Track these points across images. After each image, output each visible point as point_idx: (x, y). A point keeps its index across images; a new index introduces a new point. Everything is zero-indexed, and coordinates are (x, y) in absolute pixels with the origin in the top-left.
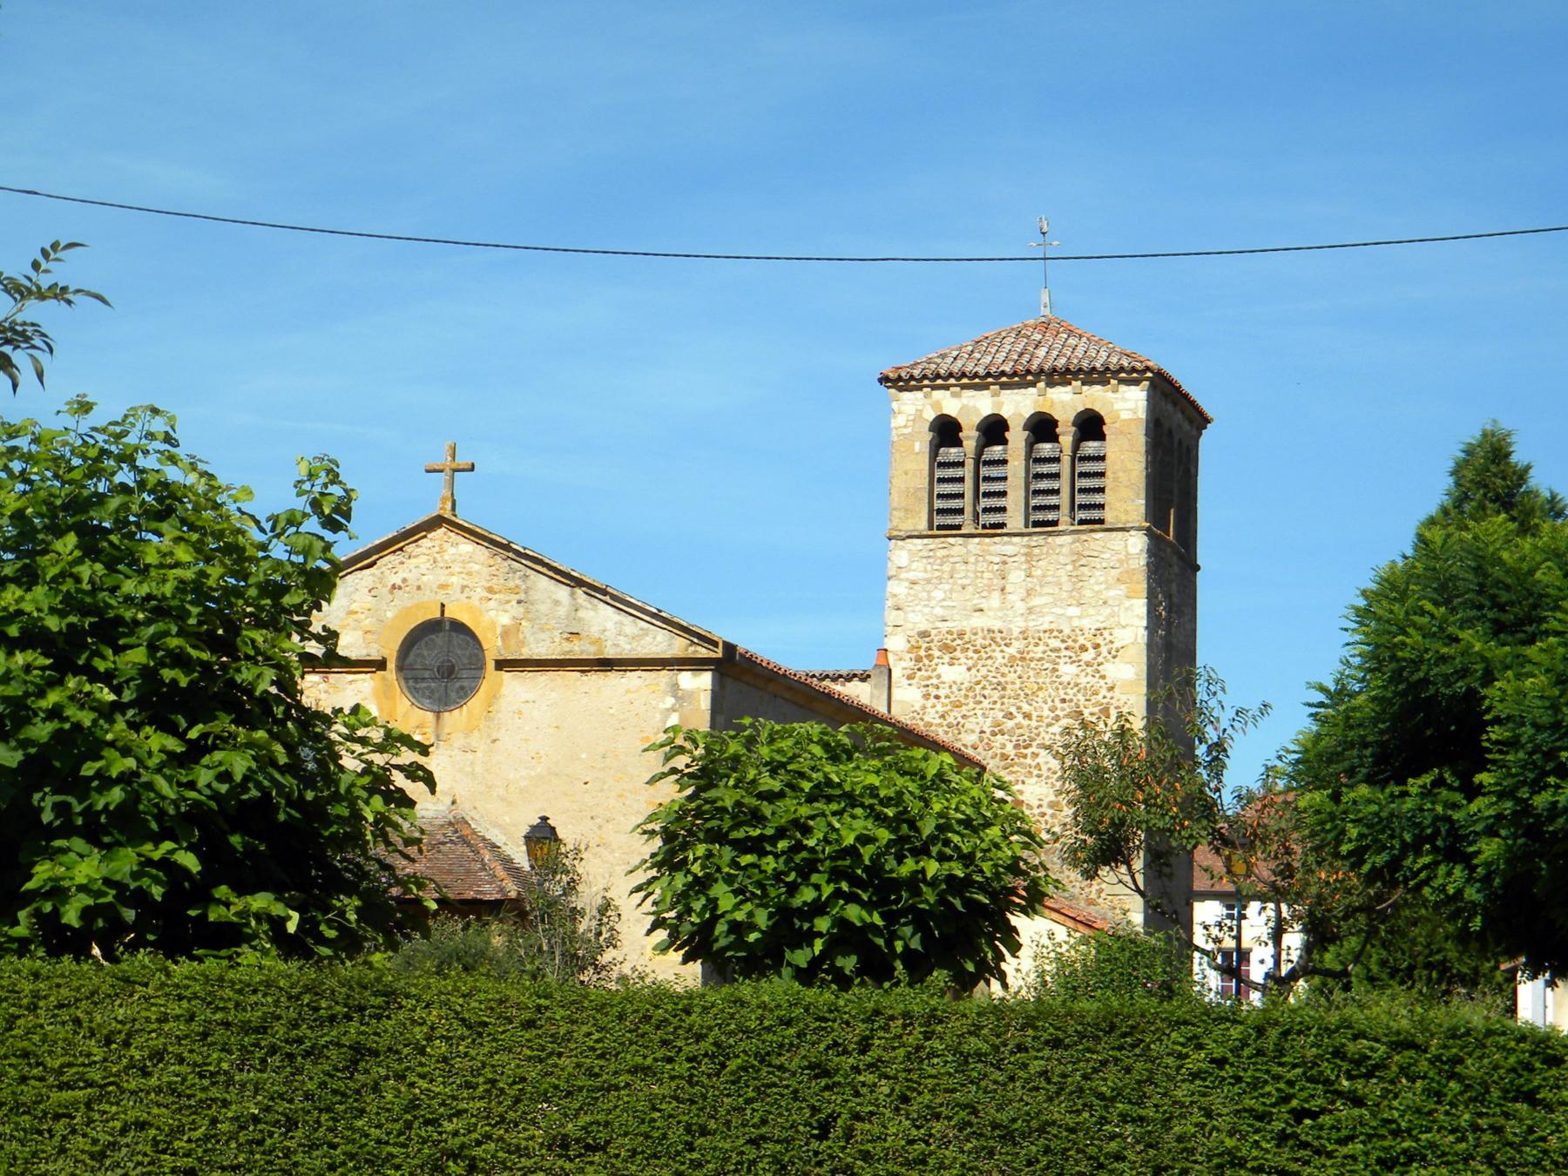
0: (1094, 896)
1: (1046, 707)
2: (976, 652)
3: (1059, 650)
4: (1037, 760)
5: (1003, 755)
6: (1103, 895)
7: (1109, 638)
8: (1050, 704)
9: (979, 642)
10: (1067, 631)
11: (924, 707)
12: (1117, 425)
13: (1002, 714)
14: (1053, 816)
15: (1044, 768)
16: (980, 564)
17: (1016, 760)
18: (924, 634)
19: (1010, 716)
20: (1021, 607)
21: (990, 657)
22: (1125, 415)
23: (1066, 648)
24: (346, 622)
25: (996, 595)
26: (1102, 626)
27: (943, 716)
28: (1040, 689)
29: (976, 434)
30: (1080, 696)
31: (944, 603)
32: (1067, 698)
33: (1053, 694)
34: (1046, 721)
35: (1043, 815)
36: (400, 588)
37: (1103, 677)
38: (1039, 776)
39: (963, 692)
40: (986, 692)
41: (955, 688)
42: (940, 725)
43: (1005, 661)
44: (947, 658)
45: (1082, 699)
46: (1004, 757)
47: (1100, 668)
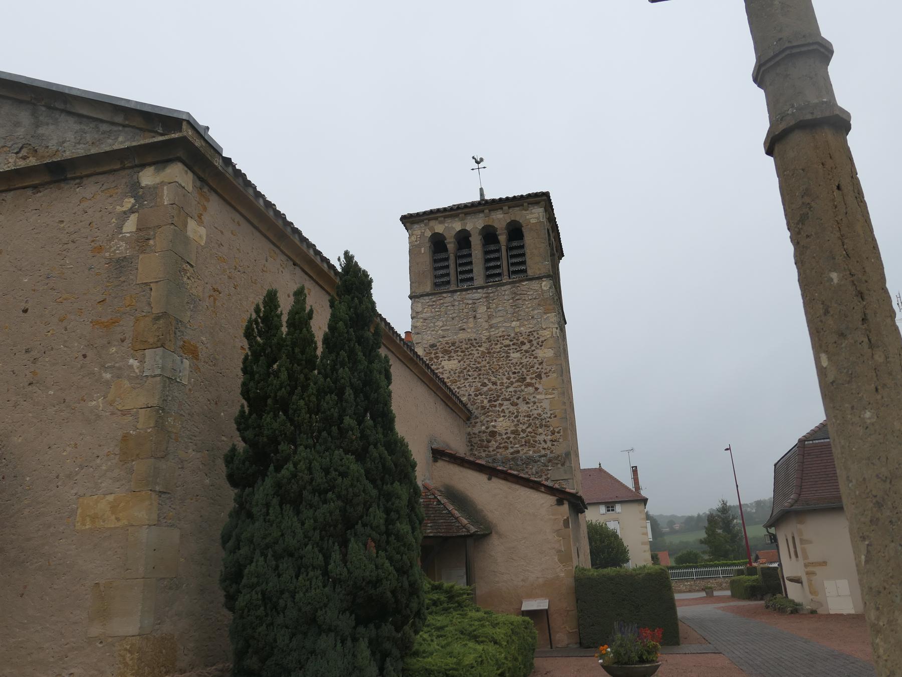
1: (504, 378)
2: (462, 352)
3: (509, 346)
4: (503, 407)
8: (507, 375)
10: (513, 335)
12: (529, 226)
13: (480, 384)
14: (515, 438)
15: (507, 411)
16: (461, 306)
18: (433, 346)
19: (484, 385)
20: (486, 326)
22: (533, 221)
23: (513, 344)
25: (471, 320)
26: (530, 330)
28: (501, 368)
29: (453, 240)
30: (523, 369)
32: (516, 371)
33: (508, 370)
34: (505, 385)
35: (509, 438)
37: (536, 358)
38: (504, 416)
40: (470, 373)
41: (452, 373)
43: (479, 355)
44: (446, 357)
45: (525, 371)
46: (483, 408)
47: (534, 353)
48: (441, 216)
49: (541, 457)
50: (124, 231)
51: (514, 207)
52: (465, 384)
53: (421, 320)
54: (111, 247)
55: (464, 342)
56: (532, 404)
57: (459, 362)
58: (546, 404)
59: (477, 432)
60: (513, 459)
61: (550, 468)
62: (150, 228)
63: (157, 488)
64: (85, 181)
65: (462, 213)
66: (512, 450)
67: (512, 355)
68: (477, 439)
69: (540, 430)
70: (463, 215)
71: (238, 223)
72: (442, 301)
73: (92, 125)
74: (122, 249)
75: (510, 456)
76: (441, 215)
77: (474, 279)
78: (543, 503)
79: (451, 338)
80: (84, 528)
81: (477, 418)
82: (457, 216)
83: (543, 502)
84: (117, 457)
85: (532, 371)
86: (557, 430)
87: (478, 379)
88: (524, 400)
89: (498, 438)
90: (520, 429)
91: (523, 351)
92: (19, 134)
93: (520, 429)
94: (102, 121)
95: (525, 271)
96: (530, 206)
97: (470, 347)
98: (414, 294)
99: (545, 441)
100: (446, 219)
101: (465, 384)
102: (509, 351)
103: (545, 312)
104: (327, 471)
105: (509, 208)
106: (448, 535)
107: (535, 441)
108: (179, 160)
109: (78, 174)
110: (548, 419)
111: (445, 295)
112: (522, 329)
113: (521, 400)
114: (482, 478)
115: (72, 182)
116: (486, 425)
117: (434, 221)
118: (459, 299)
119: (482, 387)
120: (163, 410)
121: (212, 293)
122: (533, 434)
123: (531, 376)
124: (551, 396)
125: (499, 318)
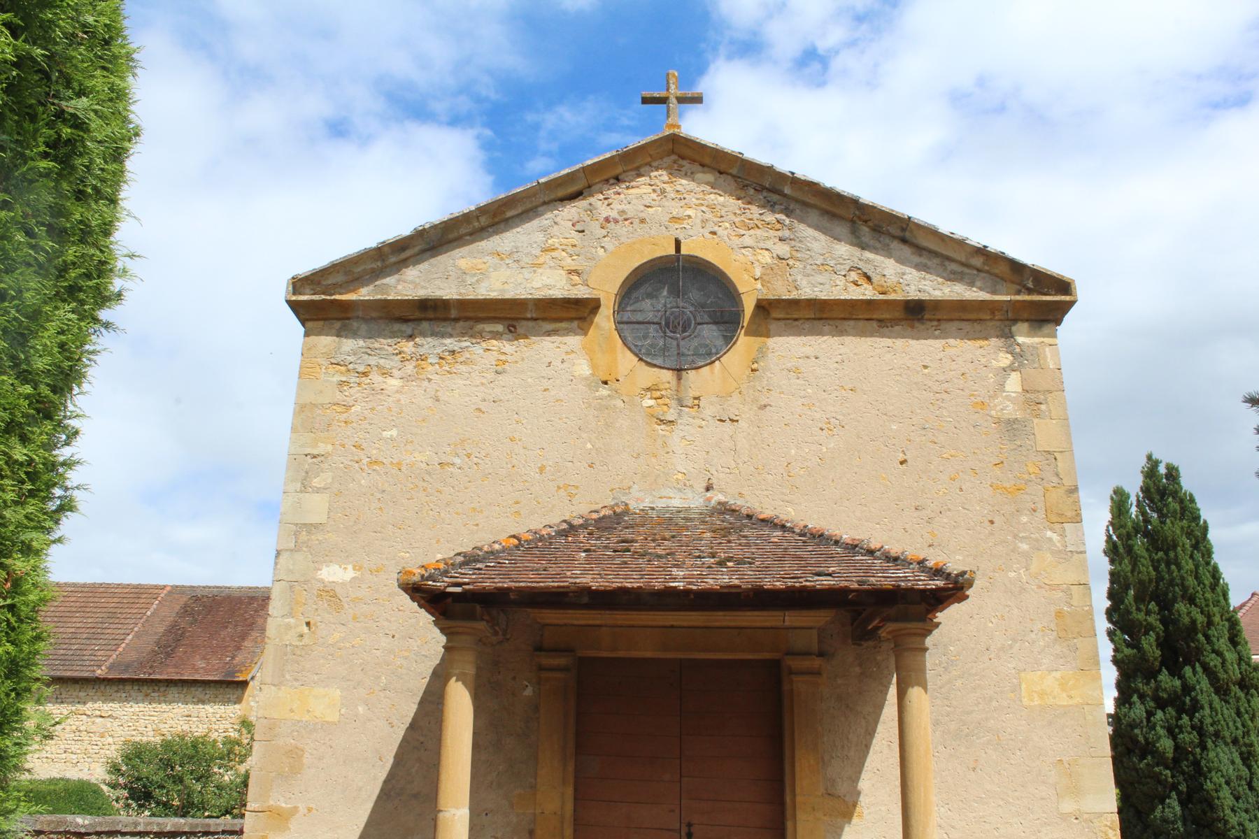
24: (541, 260)
36: (616, 221)
50: (1008, 388)
54: (995, 406)
62: (1038, 392)
64: (944, 325)
73: (936, 261)
80: (1032, 704)
84: (1055, 633)
92: (840, 253)
109: (940, 317)
115: (928, 323)
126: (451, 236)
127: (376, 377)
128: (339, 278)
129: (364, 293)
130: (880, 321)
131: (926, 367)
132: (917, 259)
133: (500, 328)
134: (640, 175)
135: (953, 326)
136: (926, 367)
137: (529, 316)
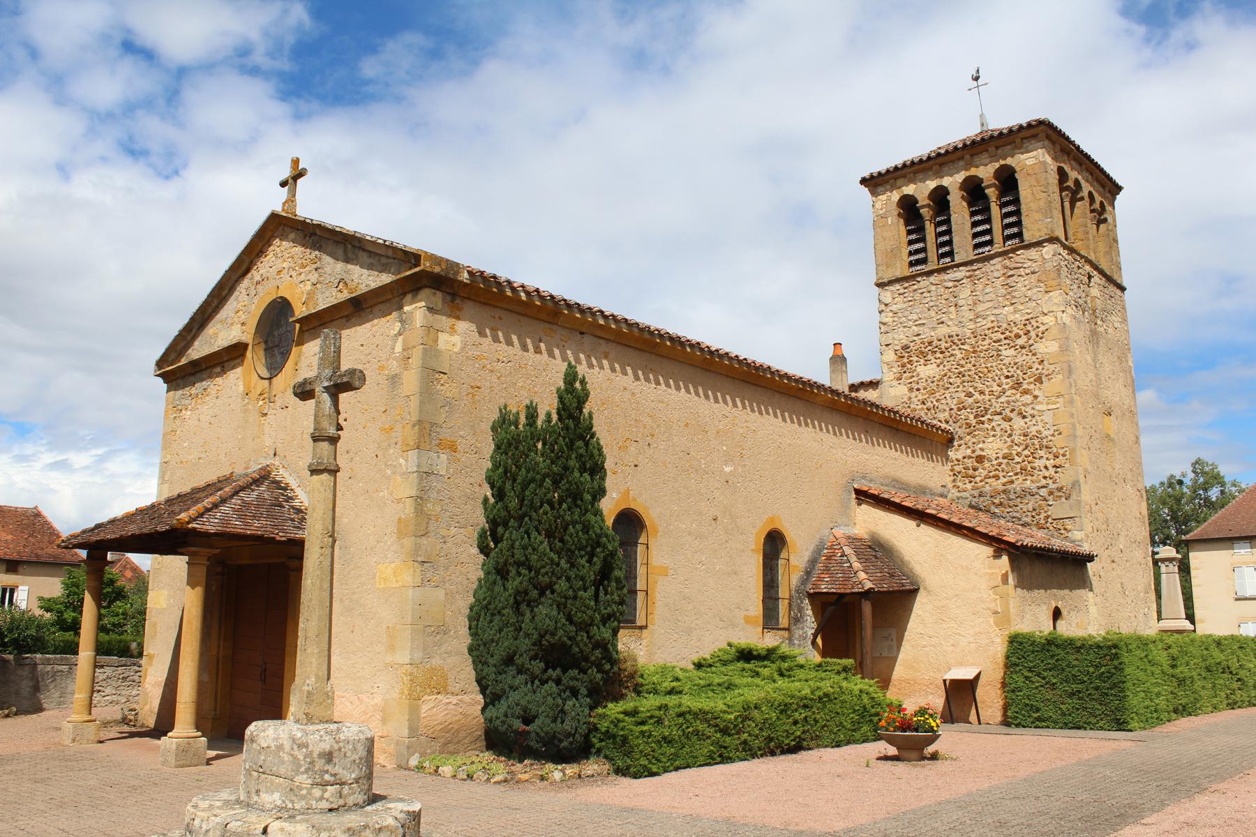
0: (1042, 522)
1: (995, 385)
2: (942, 353)
3: (999, 341)
4: (994, 424)
5: (967, 424)
6: (1050, 520)
7: (1035, 325)
8: (998, 381)
9: (943, 345)
10: (1004, 325)
11: (910, 398)
13: (964, 394)
15: (998, 429)
16: (939, 290)
17: (978, 427)
18: (905, 347)
19: (970, 395)
21: (952, 355)
23: (1005, 338)
25: (952, 309)
26: (1029, 317)
27: (923, 403)
28: (989, 371)
29: (927, 202)
30: (1019, 372)
31: (916, 323)
32: (1009, 374)
33: (999, 373)
38: (994, 436)
39: (935, 384)
40: (951, 380)
41: (929, 380)
42: (922, 409)
43: (963, 355)
44: (922, 361)
45: (1021, 374)
47: (1032, 348)
48: (910, 173)
49: (1039, 488)
51: (1004, 146)
52: (946, 395)
53: (891, 314)
55: (944, 339)
56: (1030, 418)
57: (938, 366)
58: (1048, 417)
59: (960, 457)
60: (1004, 491)
61: (1050, 503)
63: (419, 559)
65: (936, 164)
66: (1005, 480)
67: (1004, 353)
68: (961, 466)
69: (1042, 453)
70: (937, 166)
71: (500, 318)
72: (915, 287)
74: (394, 367)
75: (1001, 488)
76: (910, 170)
77: (955, 251)
78: (978, 554)
79: (927, 334)
81: (961, 438)
82: (930, 168)
83: (978, 552)
85: (1029, 373)
86: (1061, 452)
87: (961, 387)
88: (1020, 414)
89: (987, 464)
90: (1014, 452)
91: (1017, 347)
93: (1014, 452)
94: (382, 255)
95: (1019, 235)
96: (1025, 141)
97: (951, 346)
98: (880, 281)
99: (1046, 467)
100: (917, 175)
101: (946, 395)
102: (1000, 348)
103: (1047, 290)
104: (524, 548)
105: (997, 148)
106: (842, 591)
107: (1033, 468)
108: (426, 287)
110: (1050, 438)
111: (919, 279)
112: (1017, 316)
113: (1015, 412)
114: (910, 524)
116: (972, 448)
117: (902, 179)
118: (937, 282)
119: (966, 398)
120: (421, 498)
121: (470, 390)
122: (1030, 458)
123: (1028, 380)
124: (1054, 406)
125: (988, 303)
126: (206, 316)
127: (184, 412)
128: (173, 356)
129: (184, 361)
130: (347, 316)
131: (362, 345)
132: (369, 261)
133: (218, 369)
134: (270, 246)
135: (376, 309)
136: (362, 345)
137: (225, 359)
